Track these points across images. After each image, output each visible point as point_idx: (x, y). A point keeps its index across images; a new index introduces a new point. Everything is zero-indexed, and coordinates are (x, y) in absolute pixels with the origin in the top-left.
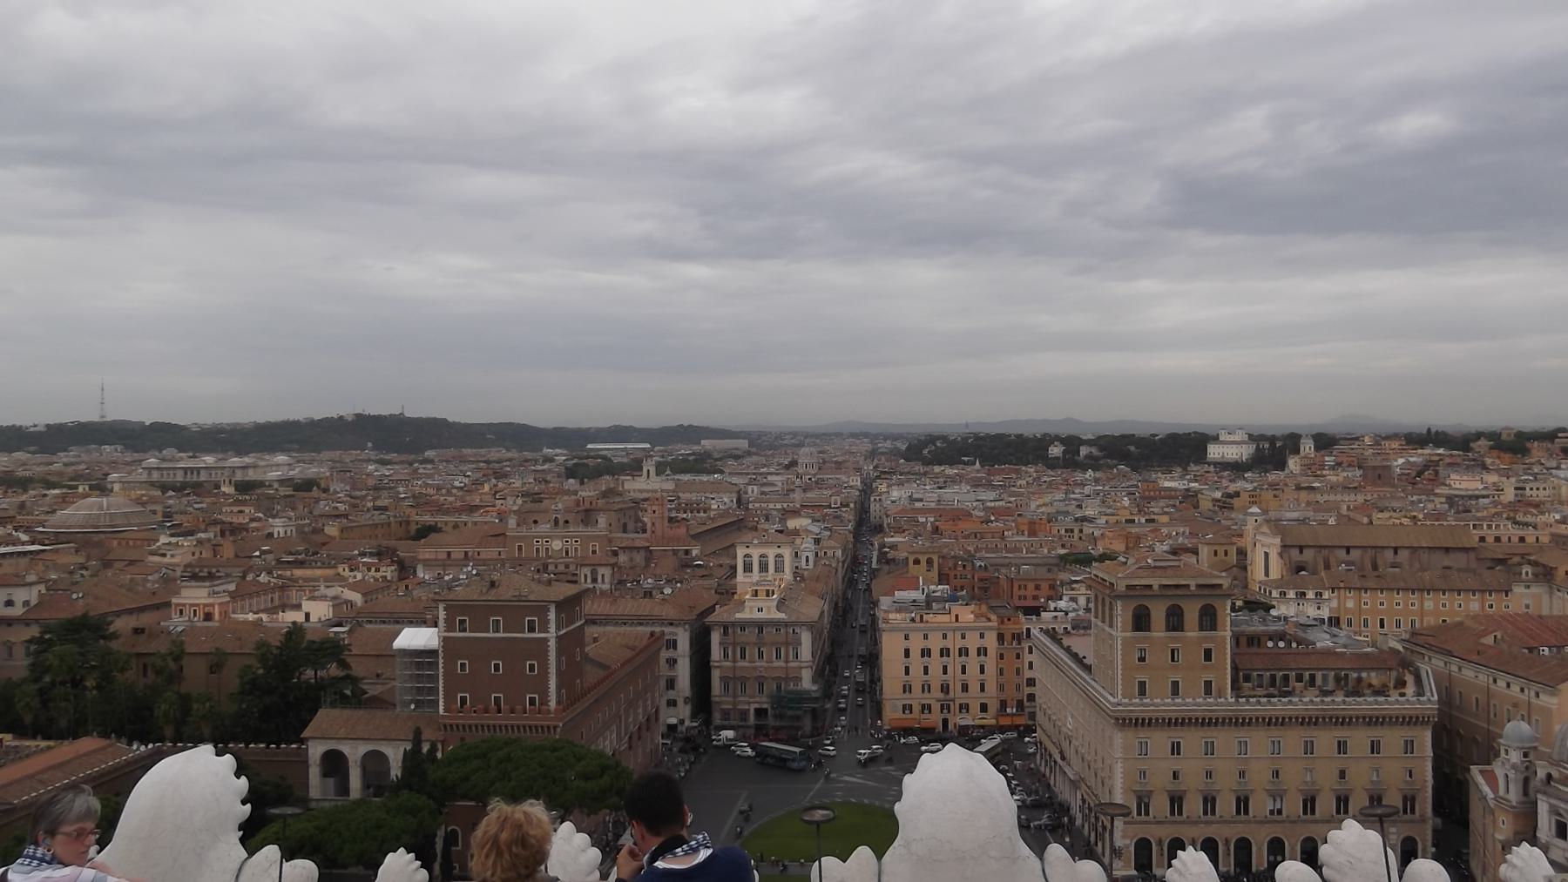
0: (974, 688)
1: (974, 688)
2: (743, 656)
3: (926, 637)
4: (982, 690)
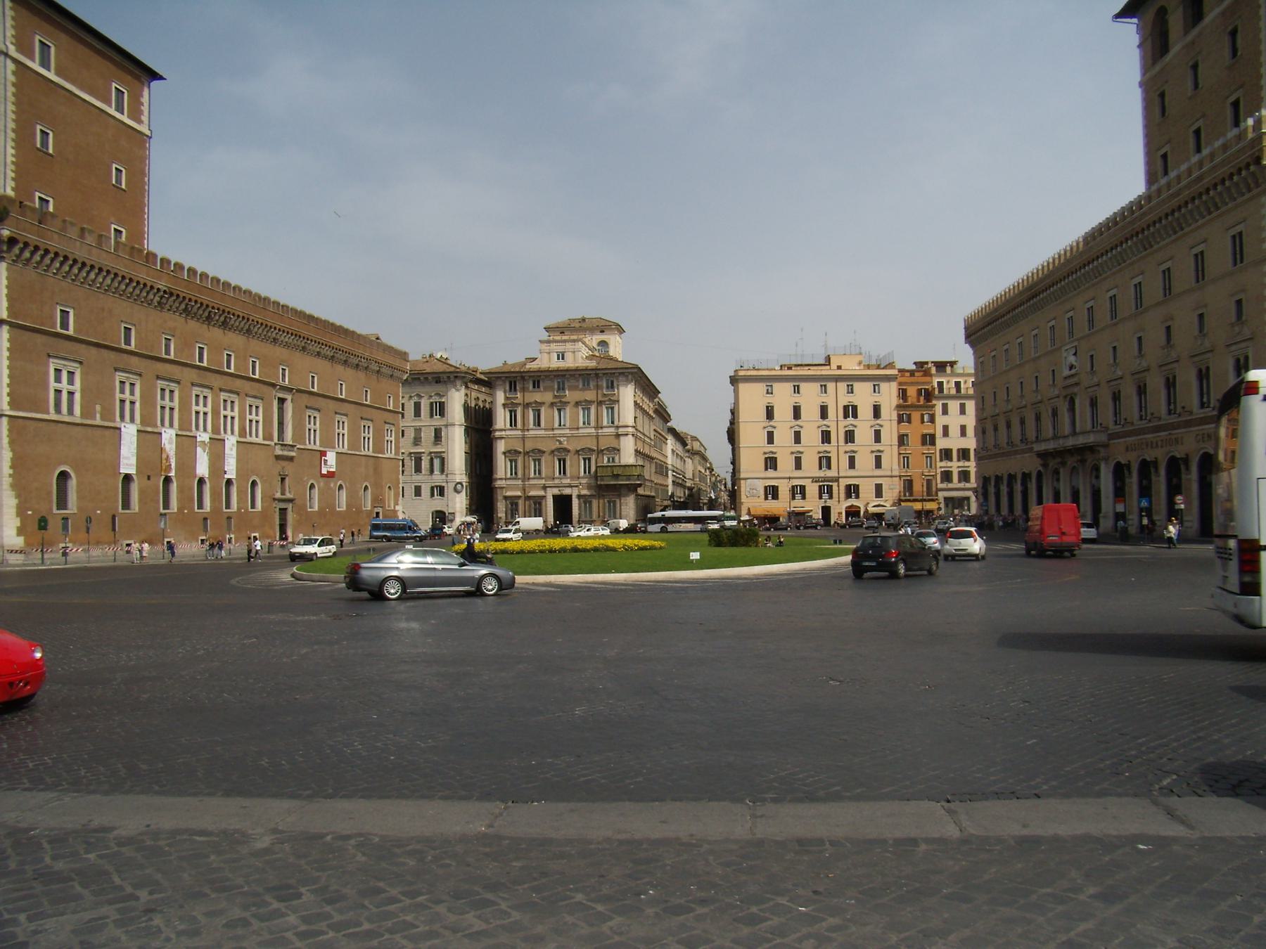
0: (865, 462)
1: (865, 462)
2: (538, 423)
3: (797, 390)
4: (878, 464)
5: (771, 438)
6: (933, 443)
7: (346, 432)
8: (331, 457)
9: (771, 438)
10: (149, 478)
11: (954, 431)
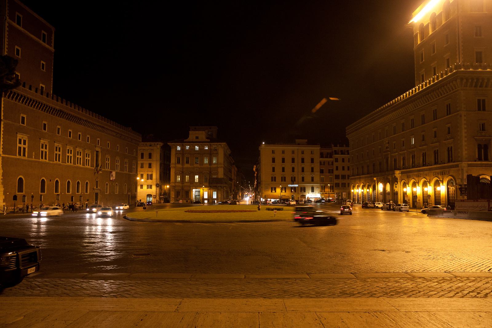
5: (274, 170)
6: (333, 173)
7: (119, 164)
8: (114, 173)
9: (274, 170)
10: (50, 181)
11: (340, 168)
